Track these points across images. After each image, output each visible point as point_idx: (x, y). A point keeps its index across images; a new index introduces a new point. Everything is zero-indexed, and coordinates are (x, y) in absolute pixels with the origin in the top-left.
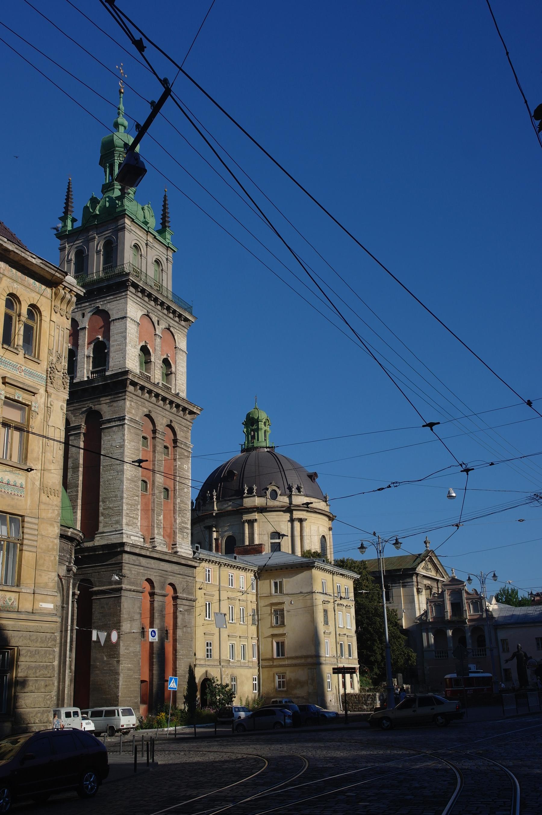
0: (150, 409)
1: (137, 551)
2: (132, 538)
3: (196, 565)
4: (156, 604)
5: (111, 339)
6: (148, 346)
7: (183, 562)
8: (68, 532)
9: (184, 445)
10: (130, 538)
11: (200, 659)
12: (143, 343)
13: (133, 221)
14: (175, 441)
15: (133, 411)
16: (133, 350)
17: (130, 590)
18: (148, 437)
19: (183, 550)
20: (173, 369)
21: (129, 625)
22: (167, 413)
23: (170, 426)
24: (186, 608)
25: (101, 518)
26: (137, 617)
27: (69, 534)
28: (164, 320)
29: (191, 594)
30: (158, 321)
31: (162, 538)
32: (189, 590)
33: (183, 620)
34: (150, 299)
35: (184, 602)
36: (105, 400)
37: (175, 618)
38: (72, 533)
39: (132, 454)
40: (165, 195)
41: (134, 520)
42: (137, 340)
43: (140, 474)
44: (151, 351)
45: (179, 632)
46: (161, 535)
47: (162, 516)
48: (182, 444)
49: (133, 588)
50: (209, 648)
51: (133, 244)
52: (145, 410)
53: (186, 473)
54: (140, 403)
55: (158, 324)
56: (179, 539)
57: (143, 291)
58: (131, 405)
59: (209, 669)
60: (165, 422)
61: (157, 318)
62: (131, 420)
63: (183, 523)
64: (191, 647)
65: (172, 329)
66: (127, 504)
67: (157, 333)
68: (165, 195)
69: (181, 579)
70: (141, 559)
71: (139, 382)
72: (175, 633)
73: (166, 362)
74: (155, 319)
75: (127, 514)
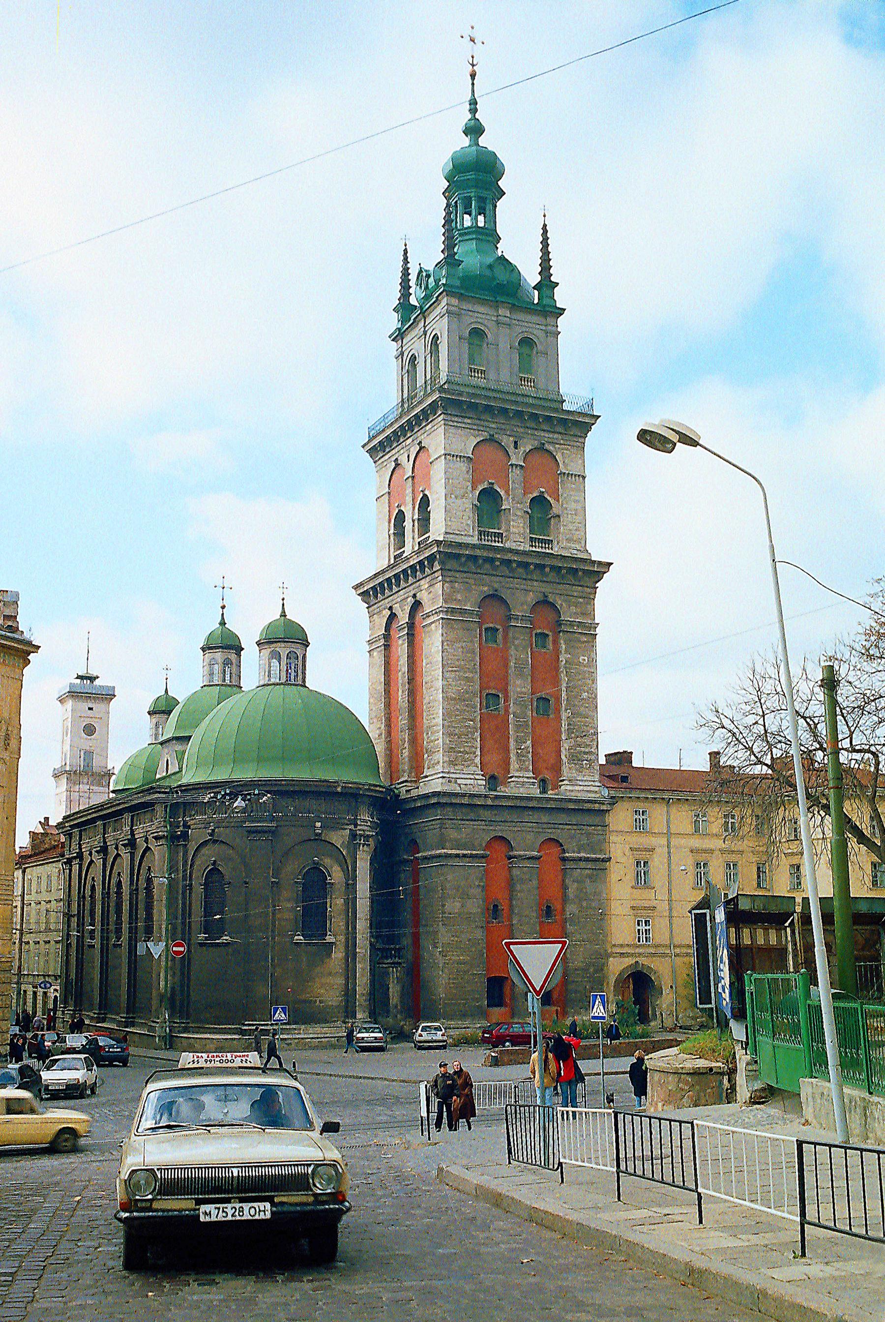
0: (496, 586)
1: (465, 801)
2: (459, 781)
3: (604, 807)
4: (516, 872)
5: (434, 489)
6: (496, 487)
7: (571, 806)
8: (336, 787)
10: (456, 782)
11: (622, 946)
12: (485, 485)
13: (461, 297)
14: (559, 623)
16: (459, 502)
17: (457, 856)
18: (498, 627)
19: (577, 788)
20: (555, 510)
21: (458, 905)
22: (535, 583)
23: (545, 603)
24: (589, 872)
25: (426, 756)
26: (476, 891)
27: (339, 789)
28: (529, 436)
29: (601, 851)
30: (516, 443)
31: (531, 775)
32: (600, 844)
34: (494, 416)
35: (582, 864)
36: (424, 584)
37: (564, 887)
39: (458, 660)
40: (545, 226)
41: (467, 756)
42: (469, 484)
43: (477, 687)
44: (502, 493)
45: (571, 909)
46: (527, 770)
47: (529, 742)
49: (465, 852)
50: (643, 927)
51: (466, 334)
52: (486, 589)
54: (472, 581)
55: (516, 448)
56: (567, 771)
57: (473, 406)
59: (642, 960)
60: (531, 598)
61: (511, 439)
62: (453, 611)
63: (579, 746)
64: (601, 928)
65: (547, 446)
66: (450, 735)
68: (545, 226)
70: (481, 811)
72: (563, 910)
73: (540, 502)
74: (507, 441)
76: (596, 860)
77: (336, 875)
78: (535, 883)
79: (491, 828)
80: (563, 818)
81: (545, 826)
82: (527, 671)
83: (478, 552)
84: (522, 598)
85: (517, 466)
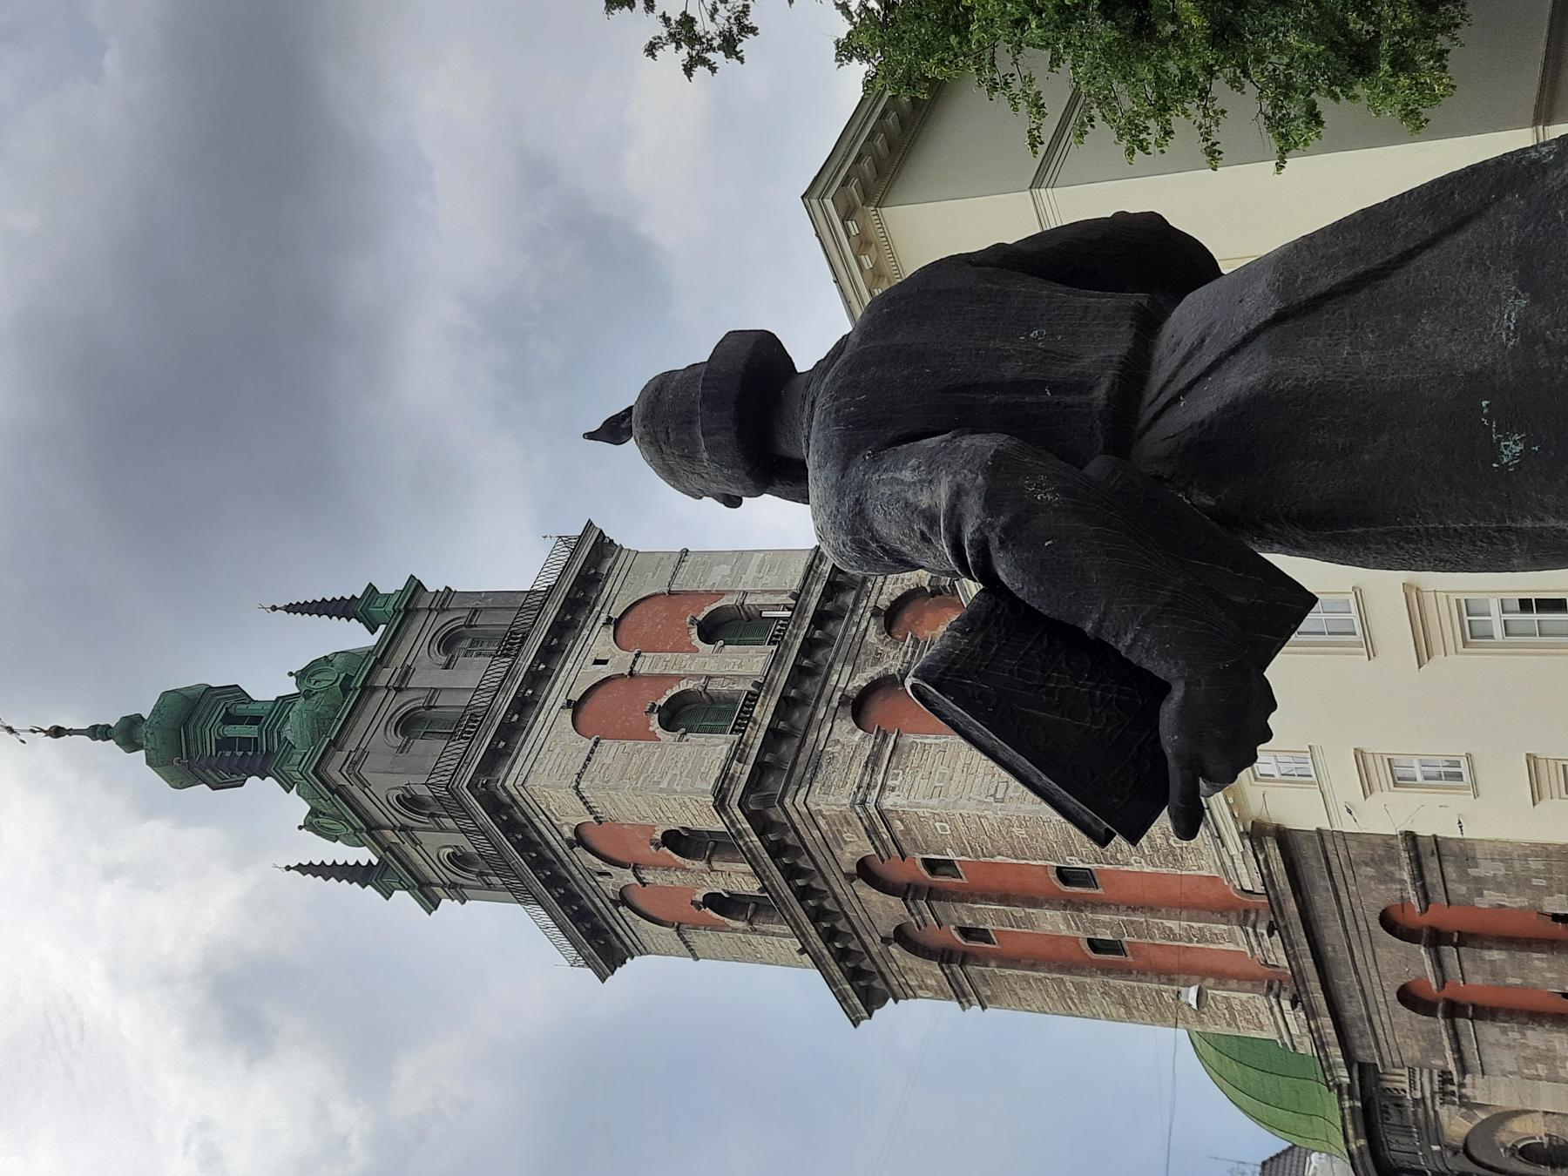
2: (1294, 1030)
9: (878, 835)
15: (931, 982)
22: (838, 890)
24: (1450, 870)
27: (1362, 1142)
33: (1499, 887)
35: (1432, 877)
38: (1357, 1137)
46: (1231, 933)
48: (882, 842)
49: (1446, 1042)
53: (963, 829)
58: (920, 988)
65: (568, 833)
67: (634, 880)
69: (1353, 888)
71: (851, 993)
75: (1229, 1025)
76: (1417, 862)
77: (1532, 1129)
78: (1496, 955)
79: (1382, 1007)
80: (1322, 902)
81: (1353, 932)
82: (1019, 912)
83: (838, 975)
84: (883, 910)
85: (639, 879)
